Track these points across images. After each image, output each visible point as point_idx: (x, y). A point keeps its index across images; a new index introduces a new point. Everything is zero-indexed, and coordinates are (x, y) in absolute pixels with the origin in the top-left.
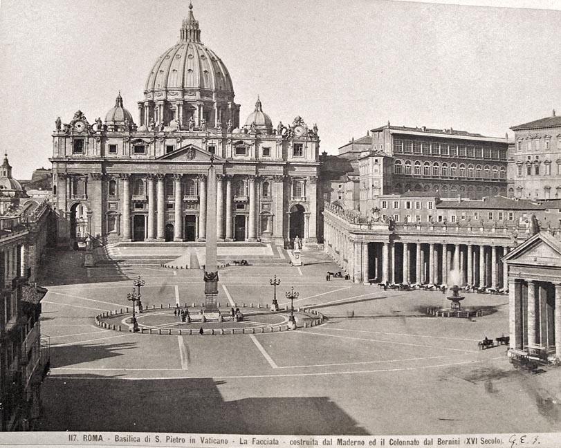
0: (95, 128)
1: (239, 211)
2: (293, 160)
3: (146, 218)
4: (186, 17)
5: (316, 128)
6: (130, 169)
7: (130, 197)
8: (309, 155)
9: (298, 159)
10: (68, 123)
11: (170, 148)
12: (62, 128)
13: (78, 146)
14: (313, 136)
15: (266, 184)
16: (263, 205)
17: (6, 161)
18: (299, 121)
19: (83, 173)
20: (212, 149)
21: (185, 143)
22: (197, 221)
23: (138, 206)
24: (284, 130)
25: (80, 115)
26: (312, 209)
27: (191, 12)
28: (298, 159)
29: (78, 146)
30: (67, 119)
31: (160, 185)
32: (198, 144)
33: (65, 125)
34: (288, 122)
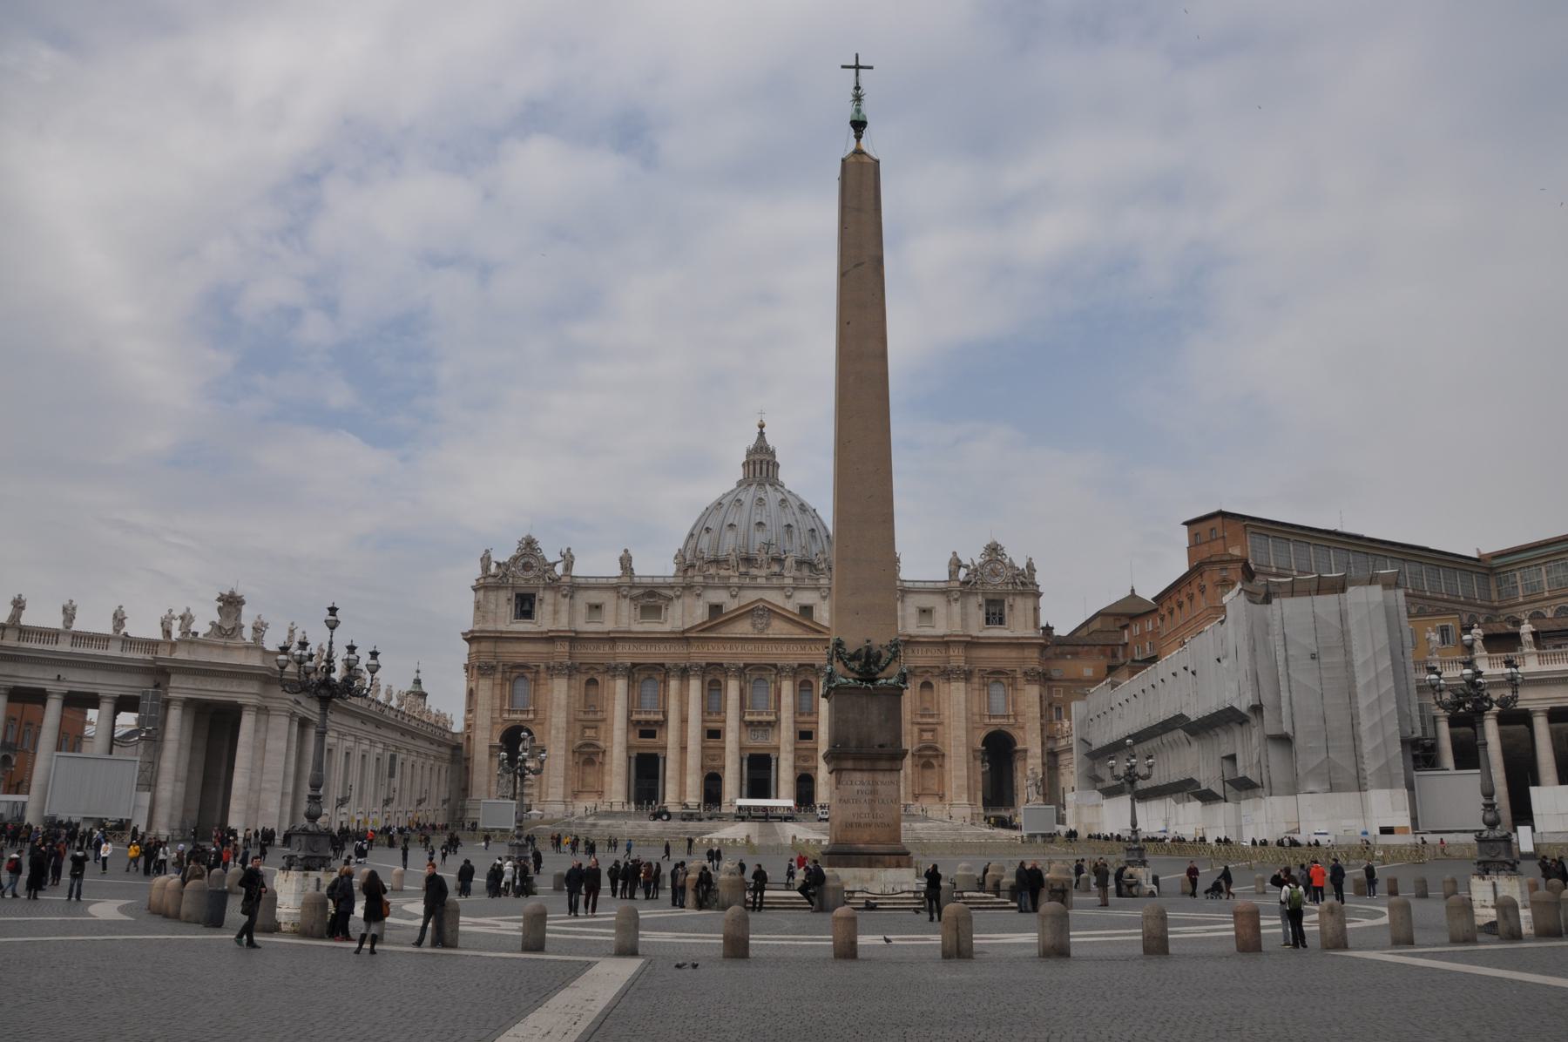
0: (559, 570)
2: (986, 633)
4: (751, 441)
5: (1030, 566)
6: (626, 654)
7: (630, 713)
8: (1017, 627)
9: (996, 632)
10: (505, 559)
11: (715, 609)
12: (493, 566)
13: (525, 606)
14: (1026, 585)
15: (927, 685)
16: (922, 730)
17: (418, 682)
18: (994, 550)
19: (532, 662)
20: (807, 610)
21: (749, 596)
23: (643, 734)
24: (962, 574)
25: (529, 545)
26: (1031, 742)
27: (761, 434)
28: (996, 632)
29: (525, 606)
30: (503, 554)
31: (695, 685)
32: (775, 598)
33: (499, 565)
34: (972, 555)
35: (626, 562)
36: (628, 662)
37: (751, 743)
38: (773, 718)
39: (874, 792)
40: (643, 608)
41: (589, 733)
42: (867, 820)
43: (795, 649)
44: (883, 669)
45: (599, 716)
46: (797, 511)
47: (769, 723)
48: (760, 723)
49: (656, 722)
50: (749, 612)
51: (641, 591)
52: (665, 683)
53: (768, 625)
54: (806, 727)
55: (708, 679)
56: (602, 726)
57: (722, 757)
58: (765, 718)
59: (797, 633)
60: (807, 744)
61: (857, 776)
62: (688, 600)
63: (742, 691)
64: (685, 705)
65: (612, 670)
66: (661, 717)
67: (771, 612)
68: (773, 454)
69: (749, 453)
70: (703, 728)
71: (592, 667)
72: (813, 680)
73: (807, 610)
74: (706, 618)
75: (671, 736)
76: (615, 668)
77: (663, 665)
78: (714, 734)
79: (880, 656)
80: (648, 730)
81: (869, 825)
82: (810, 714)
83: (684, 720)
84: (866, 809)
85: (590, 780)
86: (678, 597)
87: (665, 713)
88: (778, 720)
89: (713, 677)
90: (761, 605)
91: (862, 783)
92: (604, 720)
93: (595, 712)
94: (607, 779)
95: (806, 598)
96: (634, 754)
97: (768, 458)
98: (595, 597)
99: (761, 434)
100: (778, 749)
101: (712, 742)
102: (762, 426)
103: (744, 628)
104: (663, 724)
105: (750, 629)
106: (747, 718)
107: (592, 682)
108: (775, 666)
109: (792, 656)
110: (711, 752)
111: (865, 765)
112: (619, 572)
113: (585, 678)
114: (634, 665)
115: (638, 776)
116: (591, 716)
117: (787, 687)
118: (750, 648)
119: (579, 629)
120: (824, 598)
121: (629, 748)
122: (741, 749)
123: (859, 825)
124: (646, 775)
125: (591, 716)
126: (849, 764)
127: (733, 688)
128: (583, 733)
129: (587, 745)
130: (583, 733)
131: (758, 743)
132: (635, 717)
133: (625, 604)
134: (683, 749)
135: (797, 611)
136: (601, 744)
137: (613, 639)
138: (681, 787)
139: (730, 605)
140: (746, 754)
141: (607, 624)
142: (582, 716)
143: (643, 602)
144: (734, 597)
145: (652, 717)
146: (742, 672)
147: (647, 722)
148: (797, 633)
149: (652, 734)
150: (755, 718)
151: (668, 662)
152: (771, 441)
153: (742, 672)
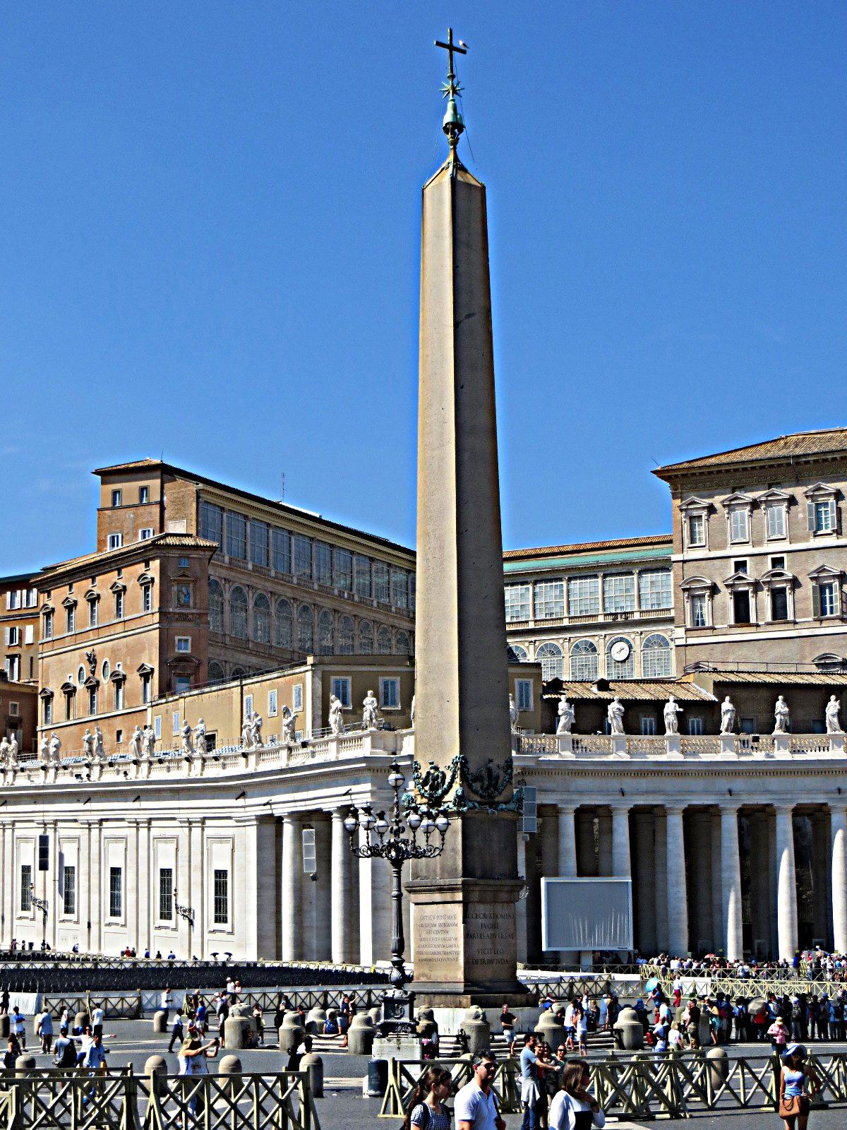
39: (495, 926)
44: (500, 793)
79: (498, 777)
81: (490, 962)
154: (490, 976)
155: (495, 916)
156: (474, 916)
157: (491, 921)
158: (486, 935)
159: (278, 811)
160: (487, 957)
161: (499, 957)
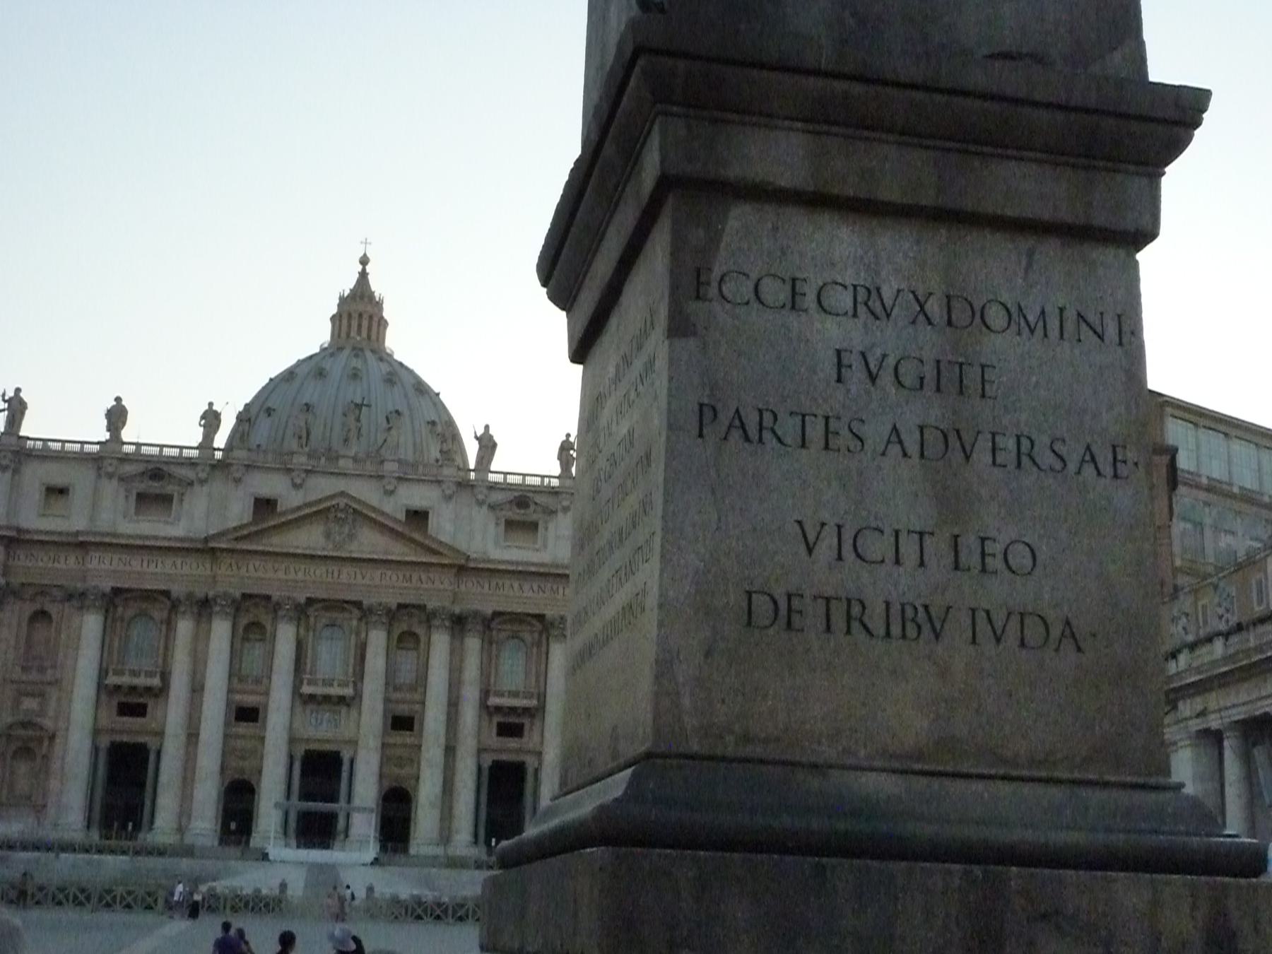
1: (509, 749)
3: (152, 757)
4: (348, 283)
6: (104, 571)
7: (103, 672)
11: (265, 506)
20: (418, 517)
21: (322, 487)
22: (345, 775)
27: (363, 275)
31: (221, 630)
32: (366, 492)
35: (117, 416)
36: (107, 585)
37: (311, 732)
38: (348, 691)
39: (955, 378)
40: (142, 498)
41: (30, 704)
42: (905, 584)
43: (393, 577)
45: (49, 675)
46: (411, 392)
47: (342, 700)
48: (327, 699)
49: (148, 690)
50: (322, 513)
51: (140, 468)
52: (169, 624)
53: (351, 537)
54: (403, 709)
55: (244, 621)
56: (53, 694)
57: (257, 754)
58: (335, 691)
59: (399, 551)
60: (406, 738)
61: (835, 250)
62: (218, 486)
63: (300, 646)
64: (202, 662)
65: (78, 598)
66: (156, 682)
67: (358, 514)
68: (379, 305)
69: (343, 301)
70: (228, 704)
71: (43, 591)
72: (420, 631)
73: (418, 517)
74: (247, 517)
75: (174, 713)
76: (83, 595)
77: (166, 593)
78: (247, 714)
80: (134, 704)
81: (923, 622)
82: (413, 688)
83: (197, 689)
84: (899, 493)
85: (22, 785)
86: (202, 482)
87: (165, 676)
88: (358, 696)
89: (252, 615)
90: (342, 502)
91: (869, 302)
92: (56, 683)
93: (42, 670)
94: (54, 784)
95: (417, 496)
96: (104, 742)
97: (369, 308)
98: (57, 475)
99: (363, 275)
100: (354, 743)
101: (243, 728)
102: (364, 261)
103: (310, 538)
104: (161, 692)
105: (322, 541)
106: (307, 689)
107: (41, 616)
108: (358, 604)
109: (387, 589)
110: (239, 744)
111: (895, 170)
112: (105, 436)
113: (29, 608)
114: (117, 591)
115: (112, 779)
116: (34, 676)
117: (377, 640)
118: (319, 571)
119: (25, 524)
120: (448, 498)
121: (96, 732)
122: (292, 741)
123: (848, 613)
124: (125, 780)
125: (34, 676)
126: (779, 155)
127: (286, 636)
128: (17, 703)
129: (25, 725)
130: (17, 703)
131: (322, 731)
132: (112, 680)
133: (110, 489)
134: (193, 736)
135: (402, 516)
136: (48, 723)
137: (83, 545)
138: (184, 802)
139: (290, 498)
140: (299, 752)
141: (75, 519)
142: (17, 674)
143: (142, 486)
144: (296, 486)
145: (141, 681)
146: (302, 611)
147: (133, 689)
148: (399, 551)
149: (138, 710)
150: (319, 690)
151: (177, 590)
152: (376, 285)
153: (302, 611)
154: (905, 715)
155: (962, 314)
156: (775, 292)
157: (930, 343)
158: (876, 432)
159: (1214, 723)
160: (883, 586)
161: (998, 593)
